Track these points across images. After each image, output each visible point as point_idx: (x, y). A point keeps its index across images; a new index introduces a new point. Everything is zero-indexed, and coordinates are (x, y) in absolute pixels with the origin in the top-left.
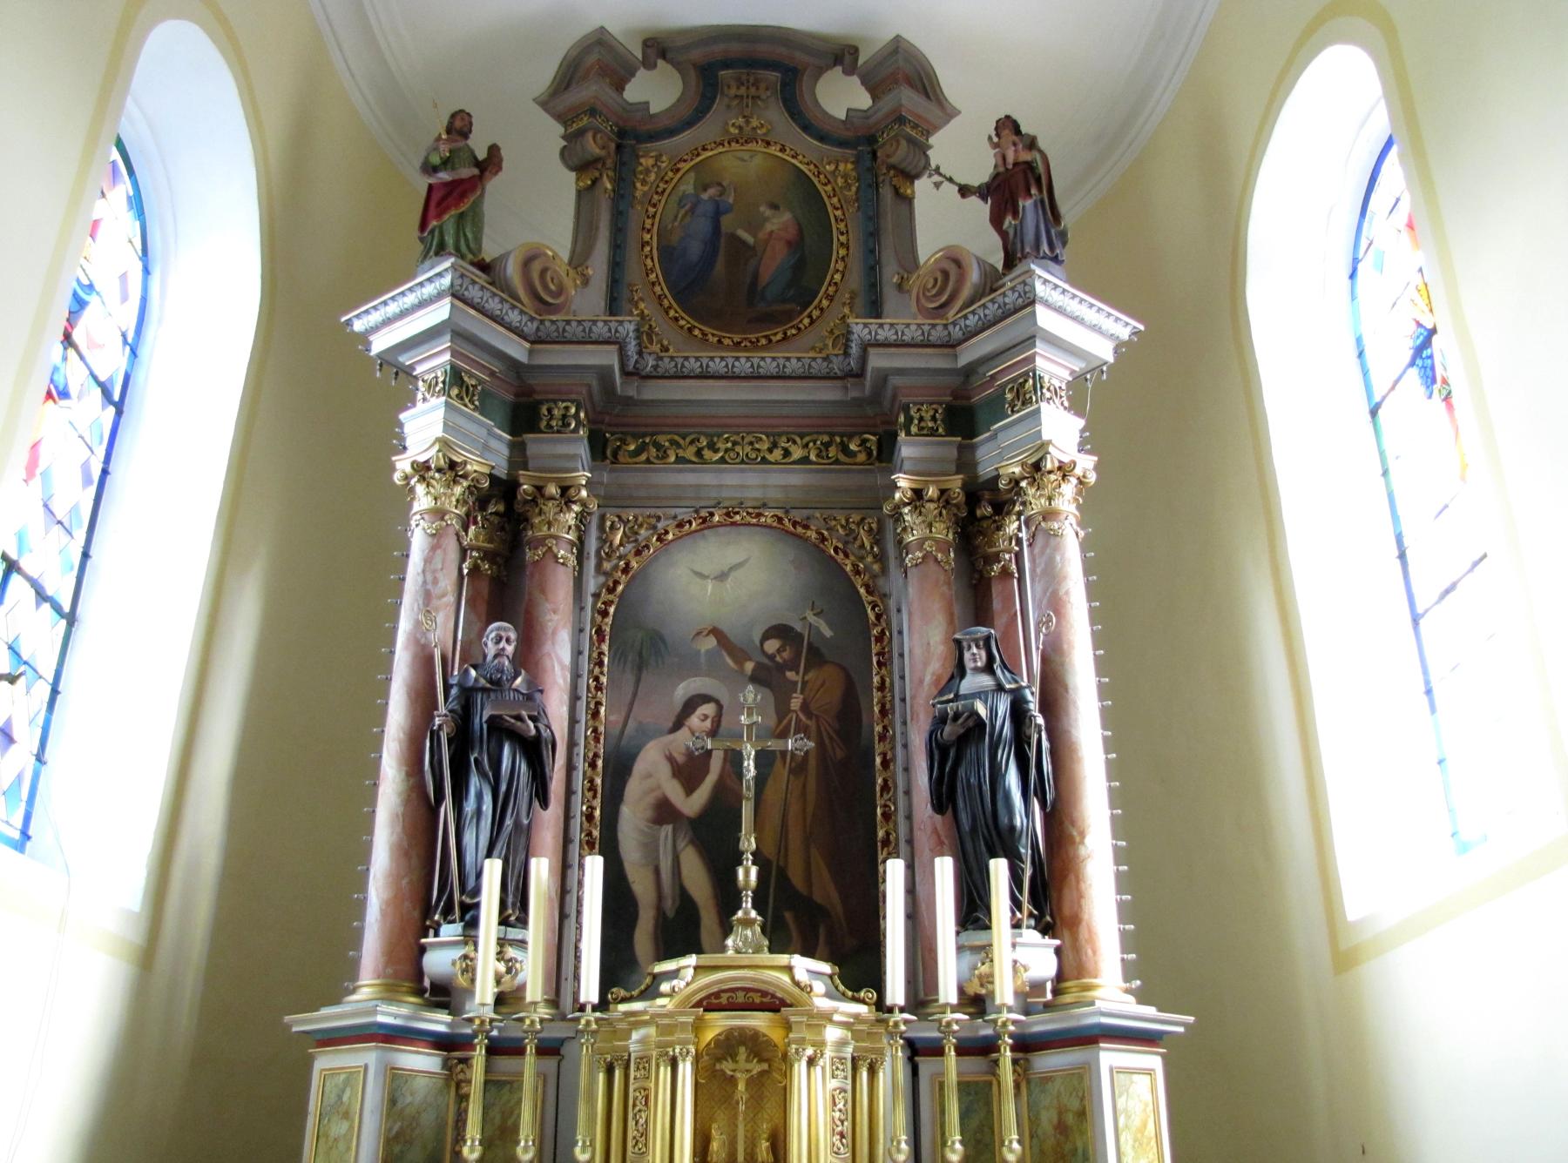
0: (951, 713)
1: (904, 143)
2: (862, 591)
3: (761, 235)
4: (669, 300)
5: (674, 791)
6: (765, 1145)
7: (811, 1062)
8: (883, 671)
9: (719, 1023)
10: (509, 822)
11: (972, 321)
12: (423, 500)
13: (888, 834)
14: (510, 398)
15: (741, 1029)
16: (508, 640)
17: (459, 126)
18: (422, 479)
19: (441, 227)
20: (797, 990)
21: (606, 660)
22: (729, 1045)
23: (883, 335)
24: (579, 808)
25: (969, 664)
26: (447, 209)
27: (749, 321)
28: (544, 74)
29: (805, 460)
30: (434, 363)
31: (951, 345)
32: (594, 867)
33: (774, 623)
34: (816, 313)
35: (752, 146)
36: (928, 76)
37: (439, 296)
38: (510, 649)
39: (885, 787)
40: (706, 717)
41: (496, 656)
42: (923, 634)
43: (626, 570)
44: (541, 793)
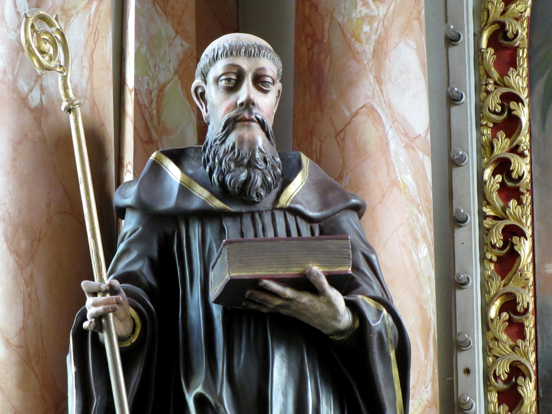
16: (259, 81)
21: (524, 114)
38: (266, 104)
41: (231, 124)
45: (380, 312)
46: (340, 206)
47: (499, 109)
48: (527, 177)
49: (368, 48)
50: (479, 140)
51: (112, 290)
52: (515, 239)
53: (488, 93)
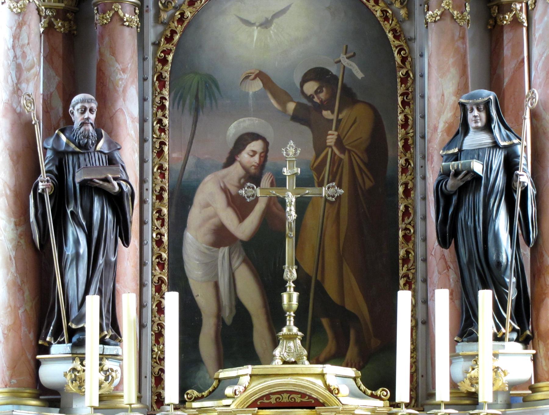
0: (453, 171)
2: (390, 36)
5: (229, 218)
8: (407, 110)
10: (101, 261)
13: (408, 253)
16: (91, 110)
20: (327, 393)
21: (167, 104)
24: (150, 235)
25: (472, 125)
32: (172, 300)
38: (93, 117)
39: (406, 213)
40: (255, 153)
41: (82, 124)
42: (441, 86)
43: (181, 21)
45: (127, 186)
46: (114, 149)
47: (159, 102)
48: (168, 125)
49: (121, 89)
50: (152, 112)
51: (48, 181)
52: (163, 146)
53: (156, 96)
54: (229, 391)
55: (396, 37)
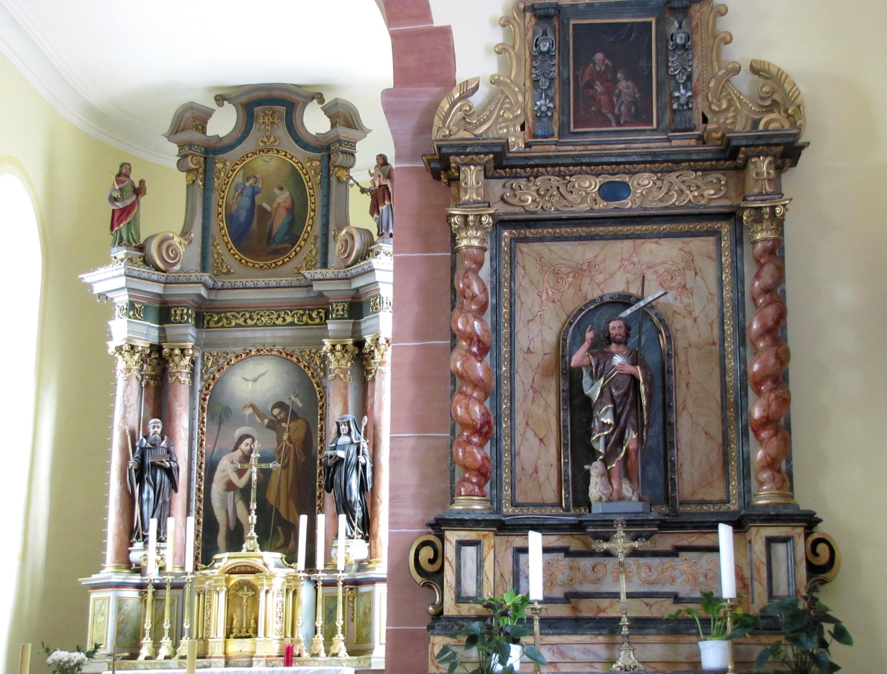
1: (340, 154)
3: (275, 205)
4: (231, 245)
5: (234, 478)
6: (253, 621)
7: (267, 592)
9: (236, 578)
10: (160, 501)
11: (354, 272)
12: (121, 365)
14: (157, 305)
15: (244, 581)
17: (123, 173)
18: (120, 354)
19: (120, 230)
22: (240, 585)
23: (317, 277)
24: (195, 486)
26: (120, 223)
27: (268, 254)
28: (166, 125)
29: (292, 324)
30: (122, 299)
31: (348, 279)
33: (277, 401)
34: (298, 249)
35: (270, 153)
36: (355, 114)
37: (121, 276)
38: (159, 431)
43: (213, 379)
44: (174, 486)
54: (216, 565)
55: (318, 386)
